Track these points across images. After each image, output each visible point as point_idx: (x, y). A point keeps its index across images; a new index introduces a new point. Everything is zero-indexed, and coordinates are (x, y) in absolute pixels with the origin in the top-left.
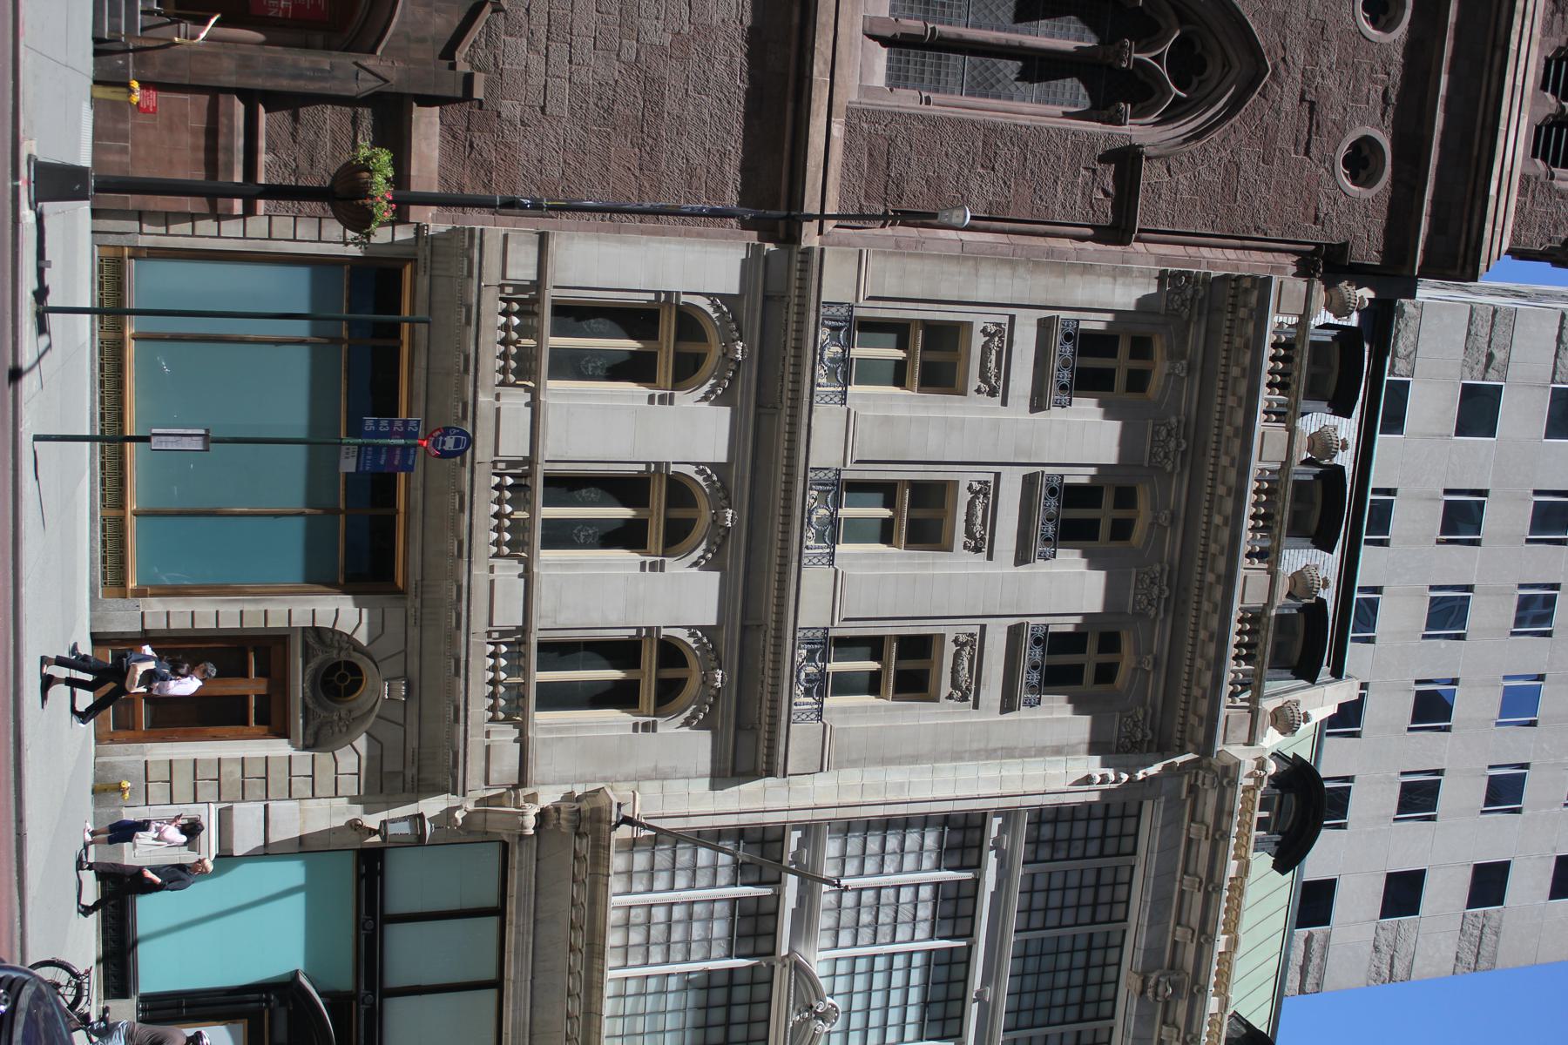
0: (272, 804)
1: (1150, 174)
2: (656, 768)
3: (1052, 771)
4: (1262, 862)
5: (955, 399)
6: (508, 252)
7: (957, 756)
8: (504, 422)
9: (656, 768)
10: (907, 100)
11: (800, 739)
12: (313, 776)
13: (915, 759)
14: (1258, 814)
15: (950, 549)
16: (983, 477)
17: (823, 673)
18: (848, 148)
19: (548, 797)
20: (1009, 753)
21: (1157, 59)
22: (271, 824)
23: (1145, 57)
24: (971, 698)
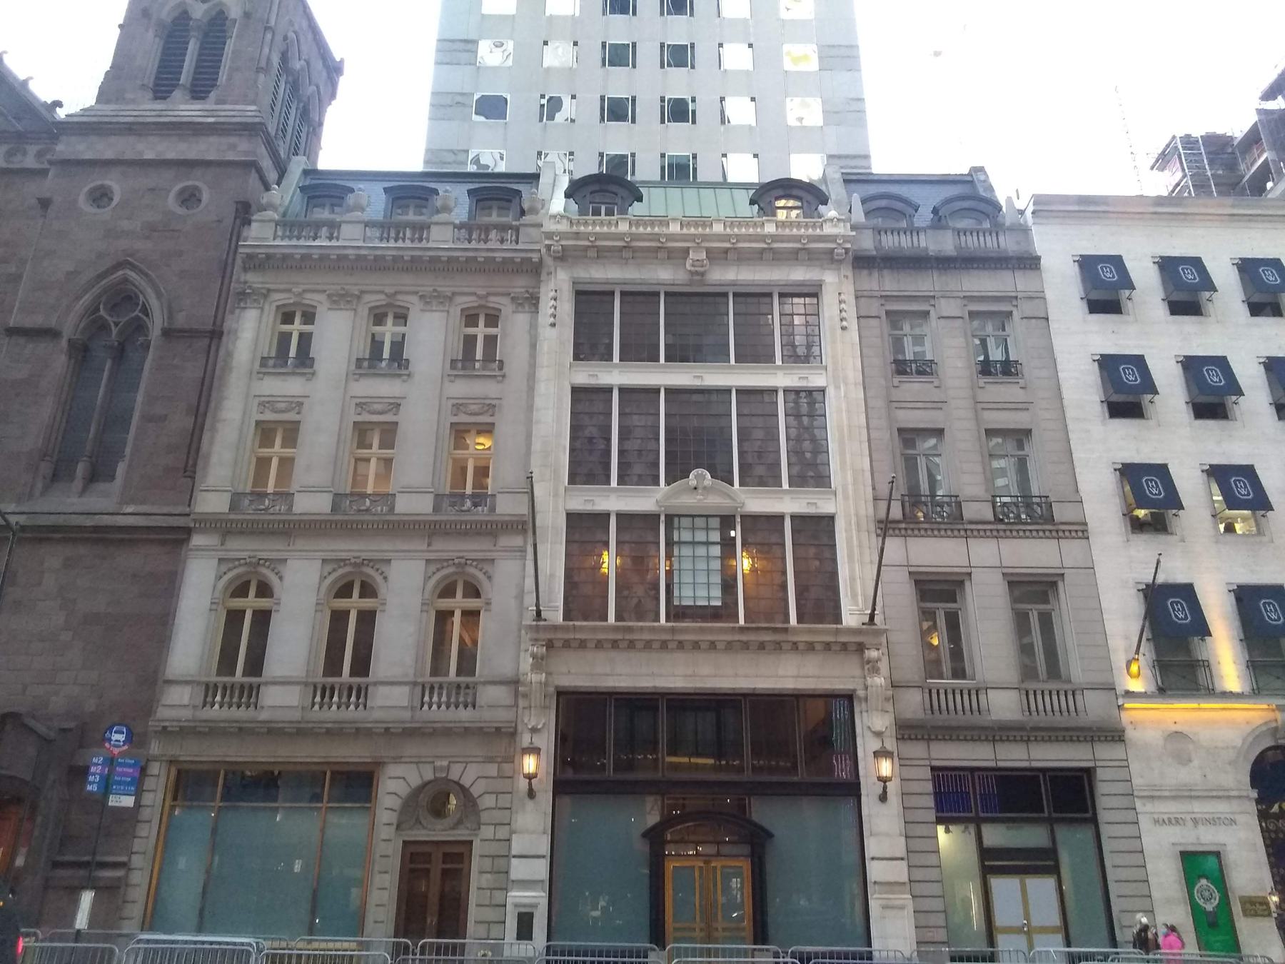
0: (514, 852)
1: (181, 320)
2: (516, 597)
3: (546, 349)
4: (637, 209)
5: (302, 427)
6: (177, 702)
7: (530, 408)
8: (280, 700)
9: (516, 597)
10: (121, 469)
11: (508, 506)
12: (495, 825)
13: (529, 436)
14: (603, 217)
15: (397, 423)
16: (353, 406)
17: (473, 496)
18: (143, 502)
19: (526, 663)
20: (531, 378)
21: (116, 324)
22: (525, 853)
23: (115, 331)
24: (493, 402)
